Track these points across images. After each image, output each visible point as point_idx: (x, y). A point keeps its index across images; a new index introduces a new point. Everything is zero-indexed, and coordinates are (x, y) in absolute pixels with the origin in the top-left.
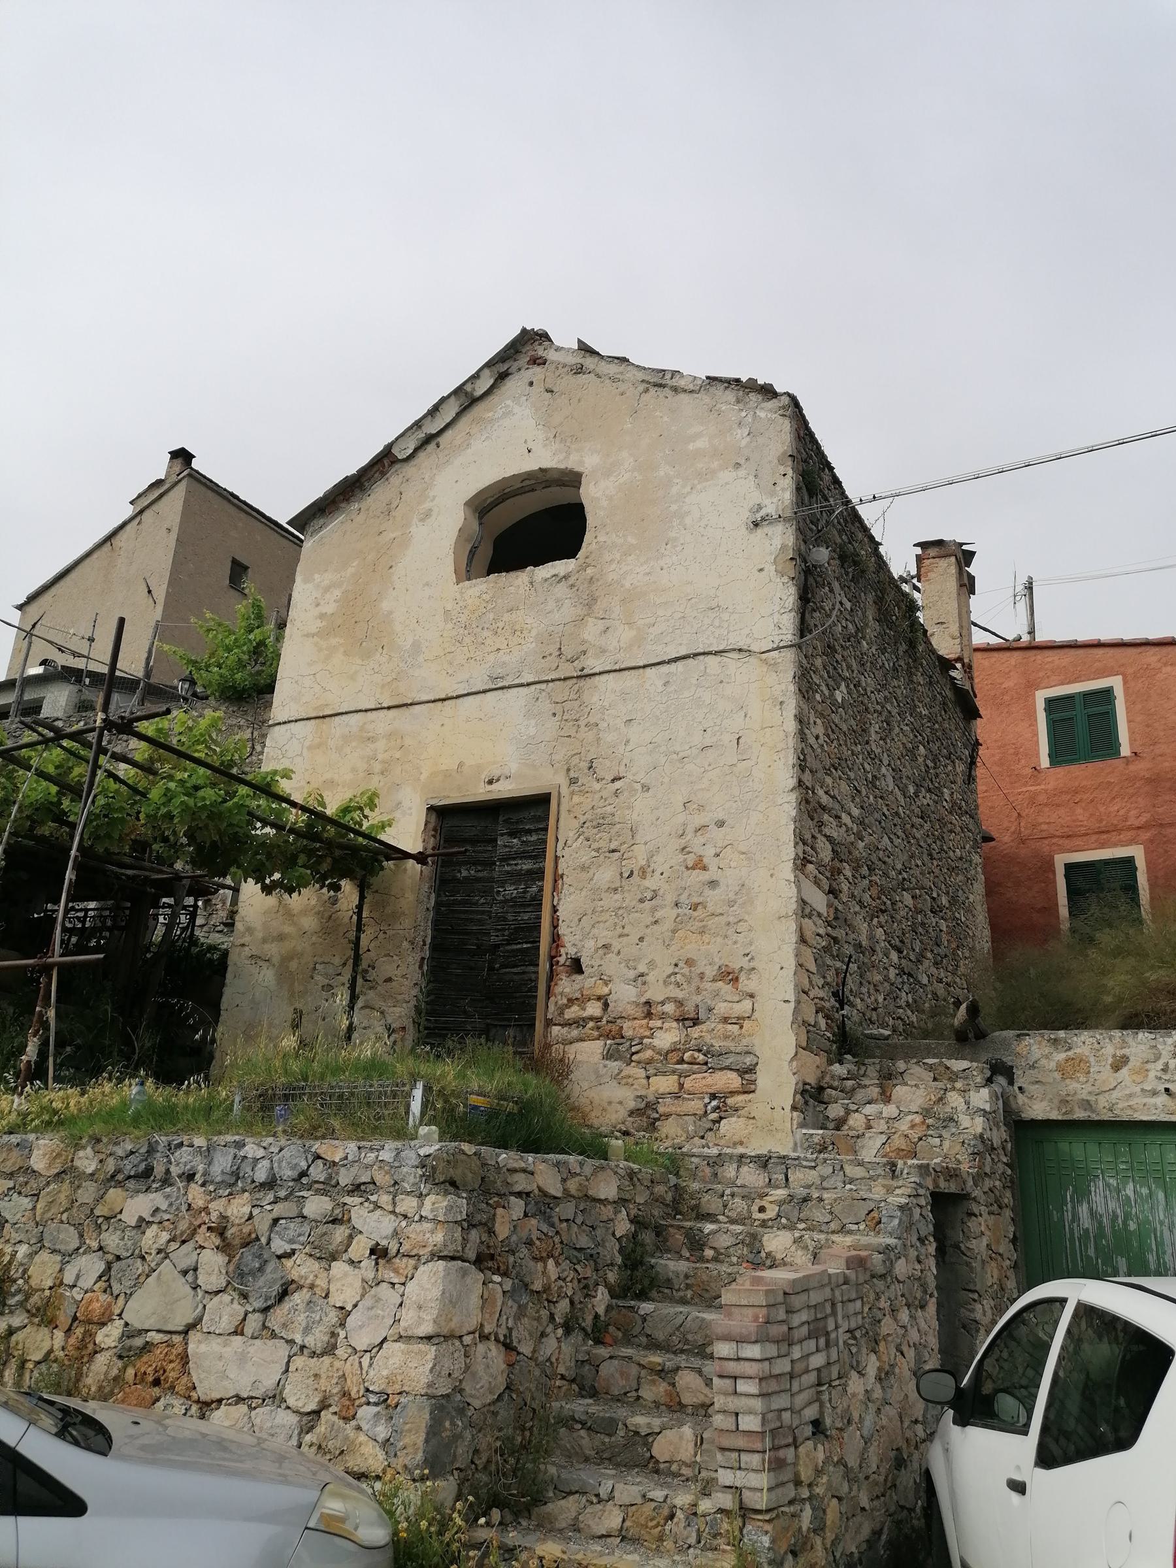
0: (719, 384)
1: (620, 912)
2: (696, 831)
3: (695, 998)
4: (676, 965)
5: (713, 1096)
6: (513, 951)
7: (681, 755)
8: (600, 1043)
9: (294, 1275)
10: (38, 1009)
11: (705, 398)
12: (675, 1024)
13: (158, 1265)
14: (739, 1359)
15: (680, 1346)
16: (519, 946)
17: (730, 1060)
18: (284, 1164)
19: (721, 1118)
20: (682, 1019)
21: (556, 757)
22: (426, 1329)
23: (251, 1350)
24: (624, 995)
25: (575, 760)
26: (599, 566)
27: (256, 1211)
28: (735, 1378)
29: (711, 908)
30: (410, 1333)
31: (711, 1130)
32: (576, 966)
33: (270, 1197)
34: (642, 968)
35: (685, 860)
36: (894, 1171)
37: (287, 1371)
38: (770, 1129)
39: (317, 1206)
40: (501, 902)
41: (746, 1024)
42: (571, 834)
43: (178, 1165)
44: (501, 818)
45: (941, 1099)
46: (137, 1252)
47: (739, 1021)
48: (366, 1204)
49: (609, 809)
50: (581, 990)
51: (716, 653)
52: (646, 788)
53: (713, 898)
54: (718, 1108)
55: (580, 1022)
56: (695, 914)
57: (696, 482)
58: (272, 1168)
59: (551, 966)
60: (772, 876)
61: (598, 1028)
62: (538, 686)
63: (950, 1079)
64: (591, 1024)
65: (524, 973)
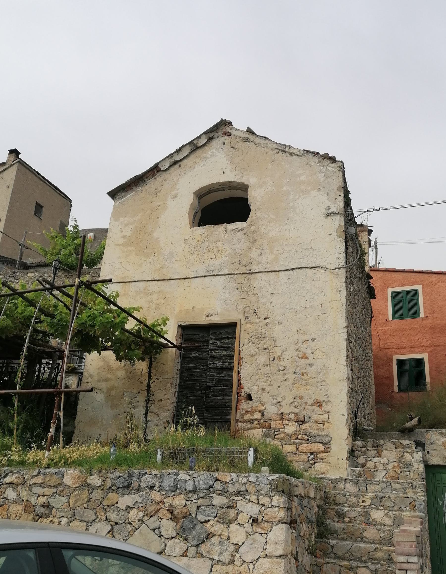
0: (310, 154)
1: (269, 375)
2: (303, 342)
3: (303, 412)
4: (295, 398)
5: (312, 454)
6: (217, 389)
7: (296, 310)
8: (260, 430)
9: (212, 531)
10: (55, 412)
11: (304, 159)
12: (294, 423)
13: (139, 527)
14: (408, 563)
15: (350, 557)
16: (220, 388)
17: (319, 439)
18: (201, 482)
19: (315, 463)
20: (297, 421)
21: (239, 307)
22: (280, 552)
23: (192, 563)
24: (271, 410)
25: (248, 309)
26: (257, 226)
27: (188, 503)
28: (406, 570)
29: (310, 375)
30: (272, 554)
31: (311, 467)
32: (249, 397)
33: (195, 496)
34: (279, 399)
35: (298, 354)
36: (412, 486)
37: (211, 571)
38: (337, 467)
39: (218, 500)
40: (211, 368)
41: (326, 423)
42: (246, 341)
43: (145, 482)
44: (211, 332)
45: (402, 456)
46: (127, 521)
47: (323, 423)
48: (244, 500)
49: (263, 331)
50: (252, 407)
51: (311, 268)
52: (280, 323)
53: (311, 371)
54: (314, 458)
55: (251, 421)
56: (303, 377)
57: (301, 194)
58: (195, 484)
59: (238, 396)
60: (337, 363)
61: (259, 424)
62: (230, 276)
63: (402, 448)
64: (256, 422)
65: (223, 399)
